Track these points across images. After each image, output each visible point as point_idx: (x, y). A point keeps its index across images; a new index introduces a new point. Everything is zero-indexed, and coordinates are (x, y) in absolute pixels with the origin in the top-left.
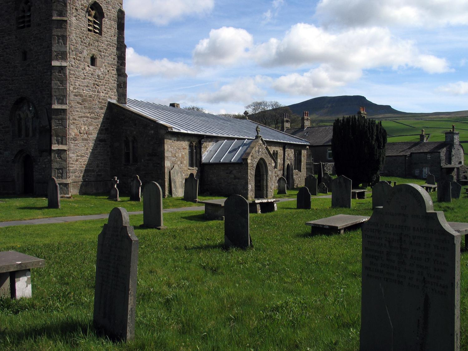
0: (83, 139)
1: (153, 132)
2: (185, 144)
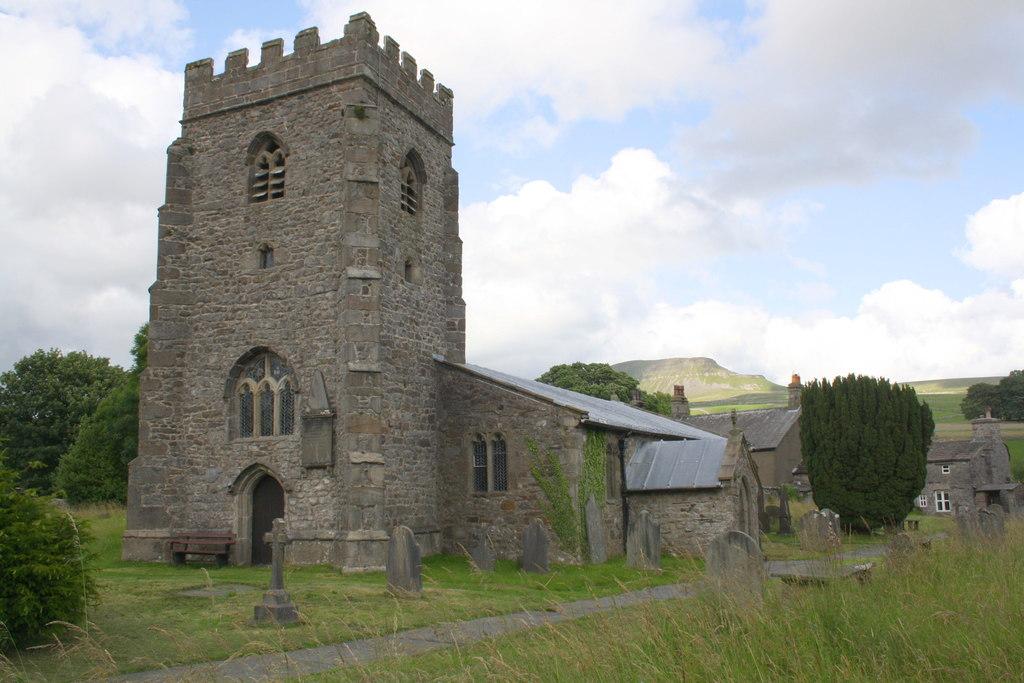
0: (395, 440)
1: (544, 423)
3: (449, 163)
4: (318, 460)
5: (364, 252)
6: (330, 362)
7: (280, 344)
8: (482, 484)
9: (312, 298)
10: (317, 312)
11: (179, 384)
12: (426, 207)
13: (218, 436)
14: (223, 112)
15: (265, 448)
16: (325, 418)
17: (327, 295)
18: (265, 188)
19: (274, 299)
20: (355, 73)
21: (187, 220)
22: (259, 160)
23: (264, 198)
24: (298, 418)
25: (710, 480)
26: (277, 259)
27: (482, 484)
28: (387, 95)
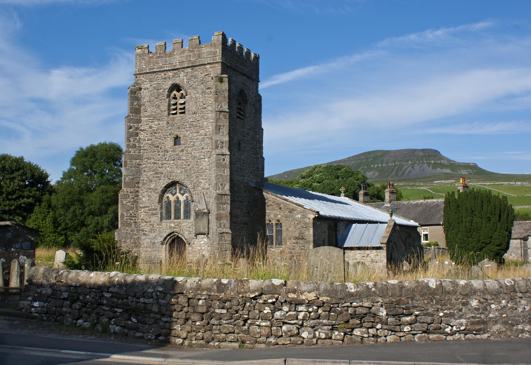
1: (300, 216)
3: (257, 91)
4: (202, 231)
5: (223, 143)
6: (207, 189)
7: (184, 180)
9: (199, 161)
10: (201, 167)
11: (137, 196)
12: (247, 115)
13: (155, 219)
14: (155, 72)
15: (178, 225)
16: (205, 213)
17: (206, 160)
18: (176, 109)
19: (181, 160)
21: (139, 121)
22: (172, 95)
23: (176, 114)
24: (193, 213)
26: (182, 142)
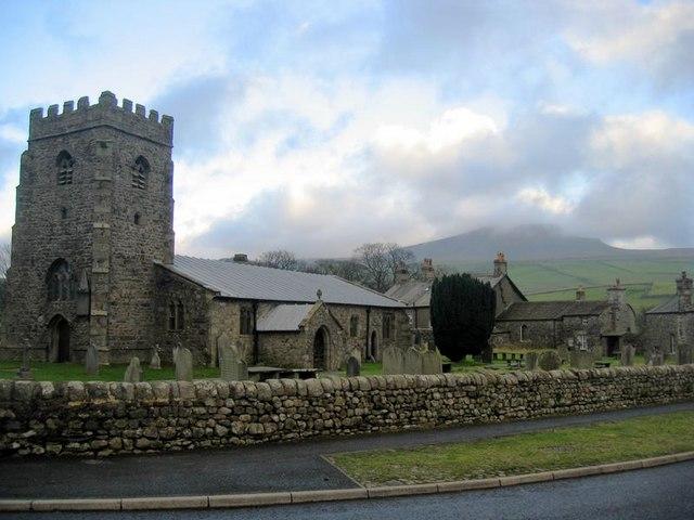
2: (236, 308)
8: (173, 326)
20: (103, 123)
22: (63, 164)
25: (296, 328)
27: (173, 326)
28: (124, 132)
